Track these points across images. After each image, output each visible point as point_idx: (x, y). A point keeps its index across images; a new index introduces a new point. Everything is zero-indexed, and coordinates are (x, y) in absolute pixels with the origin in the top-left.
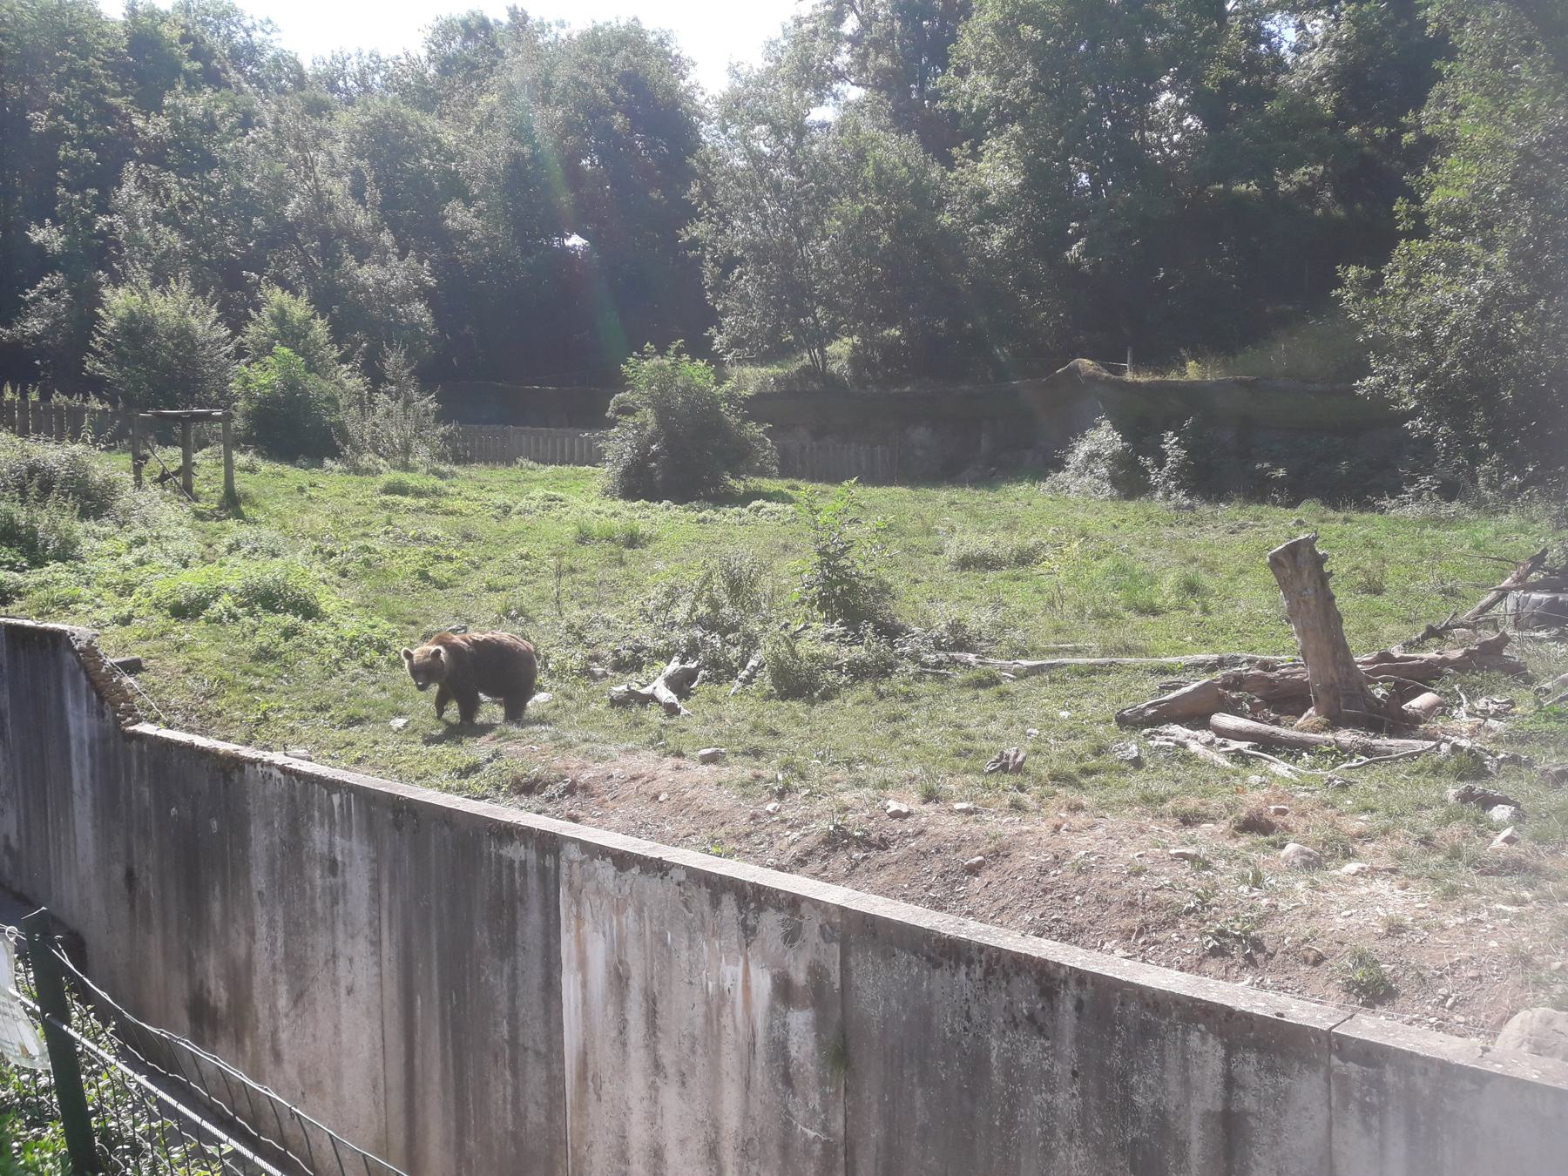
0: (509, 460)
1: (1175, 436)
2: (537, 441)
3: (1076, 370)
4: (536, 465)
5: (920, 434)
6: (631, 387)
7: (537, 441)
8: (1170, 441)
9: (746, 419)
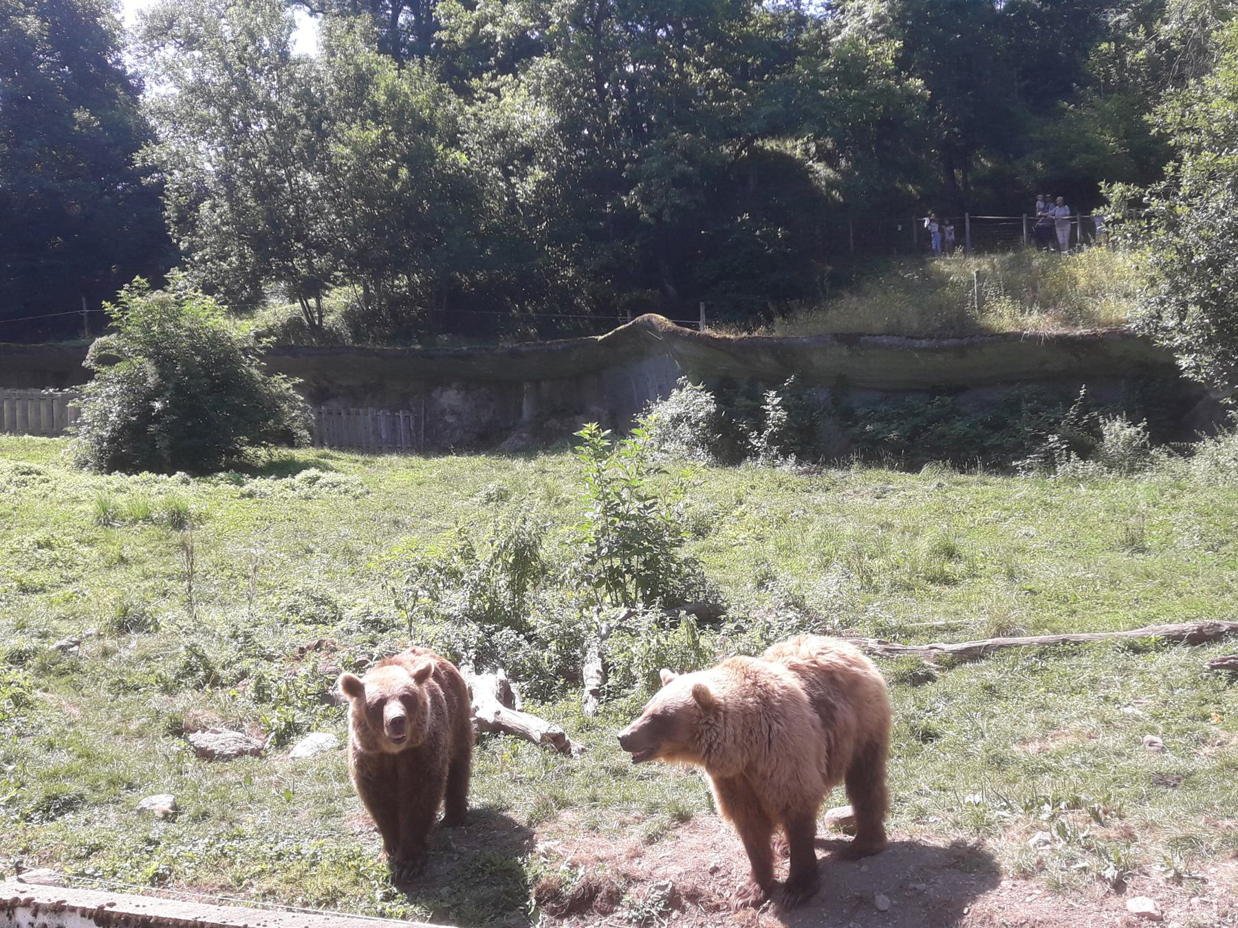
1: (777, 396)
8: (772, 399)
9: (269, 372)
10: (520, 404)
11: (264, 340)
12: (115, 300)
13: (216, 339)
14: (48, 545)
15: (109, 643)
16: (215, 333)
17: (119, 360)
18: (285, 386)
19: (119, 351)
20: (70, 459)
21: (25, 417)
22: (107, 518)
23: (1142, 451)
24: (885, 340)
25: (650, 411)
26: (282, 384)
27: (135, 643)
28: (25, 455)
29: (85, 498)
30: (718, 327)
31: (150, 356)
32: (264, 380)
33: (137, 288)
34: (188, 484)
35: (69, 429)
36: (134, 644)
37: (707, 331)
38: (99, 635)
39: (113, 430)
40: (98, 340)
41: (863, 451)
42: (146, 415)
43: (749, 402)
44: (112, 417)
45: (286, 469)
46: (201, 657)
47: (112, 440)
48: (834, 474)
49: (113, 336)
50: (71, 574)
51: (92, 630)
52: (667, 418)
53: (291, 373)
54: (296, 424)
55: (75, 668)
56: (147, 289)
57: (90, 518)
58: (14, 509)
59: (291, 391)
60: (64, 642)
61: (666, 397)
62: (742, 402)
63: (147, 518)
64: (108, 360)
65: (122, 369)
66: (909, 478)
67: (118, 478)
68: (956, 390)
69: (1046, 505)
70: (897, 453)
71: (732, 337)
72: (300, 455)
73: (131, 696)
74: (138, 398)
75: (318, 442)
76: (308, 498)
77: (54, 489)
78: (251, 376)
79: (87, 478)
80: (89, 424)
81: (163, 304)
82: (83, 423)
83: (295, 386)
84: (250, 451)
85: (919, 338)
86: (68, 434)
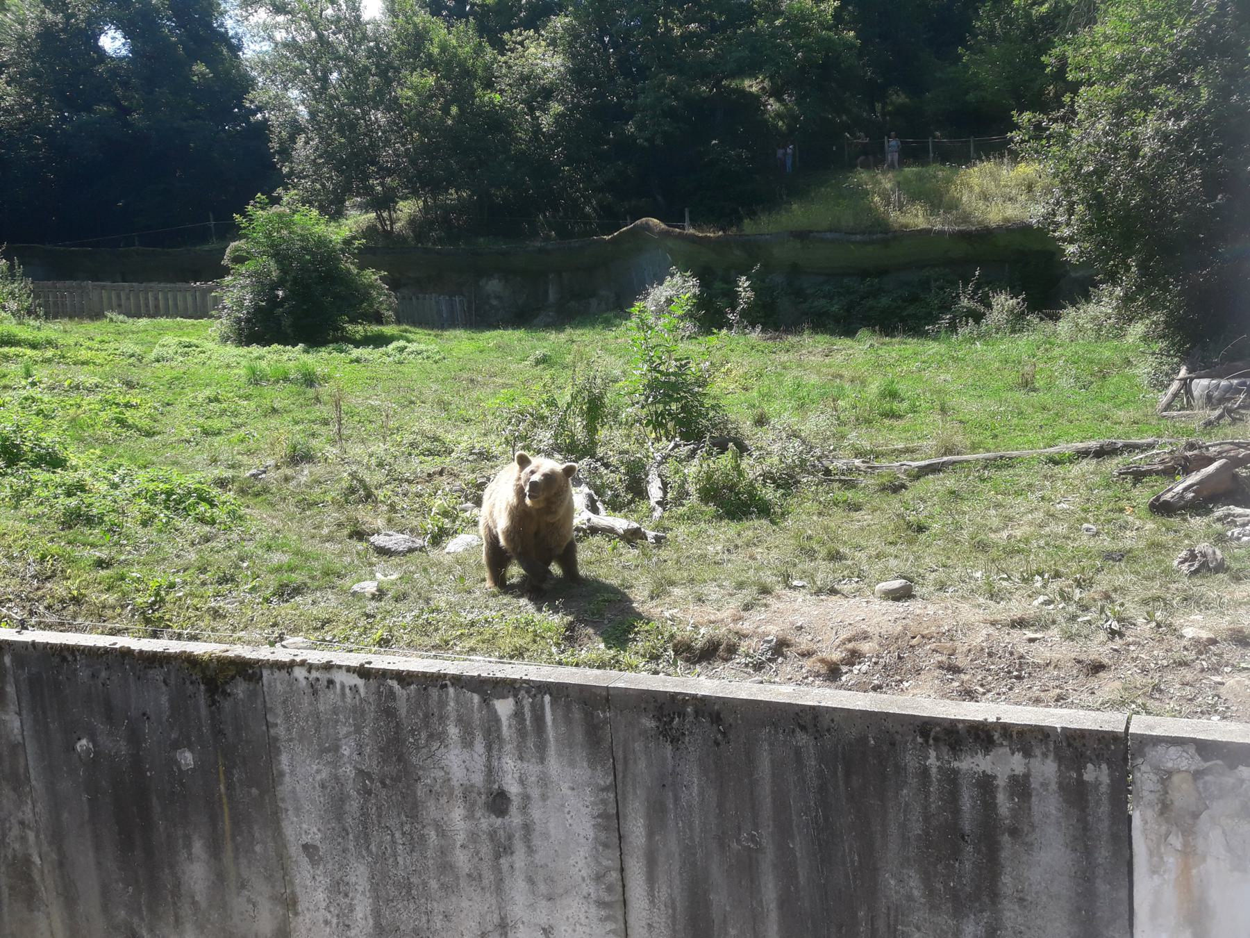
0: (97, 315)
2: (119, 297)
3: (647, 227)
4: (126, 318)
5: (493, 285)
6: (245, 236)
7: (119, 297)
8: (744, 282)
9: (362, 267)
10: (546, 292)
11: (357, 242)
12: (244, 214)
13: (322, 242)
14: (217, 400)
15: (289, 472)
16: (320, 237)
17: (248, 259)
18: (374, 277)
19: (248, 253)
20: (216, 335)
21: (176, 305)
22: (256, 379)
23: (1020, 316)
24: (829, 235)
25: (648, 294)
26: (371, 276)
27: (306, 473)
28: (180, 333)
29: (235, 364)
30: (701, 230)
31: (273, 256)
32: (358, 273)
33: (259, 203)
34: (308, 353)
35: (213, 312)
36: (306, 472)
37: (692, 231)
38: (277, 466)
39: (248, 313)
40: (233, 244)
41: (812, 322)
42: (273, 302)
43: (725, 286)
44: (247, 303)
45: (379, 341)
46: (361, 481)
47: (248, 321)
48: (792, 339)
49: (243, 241)
50: (239, 421)
51: (270, 462)
52: (663, 299)
53: (378, 269)
54: (384, 306)
55: (266, 490)
56: (267, 204)
57: (243, 379)
58: (184, 373)
59: (379, 281)
60: (254, 471)
61: (661, 284)
62: (718, 285)
63: (286, 379)
64: (239, 260)
65: (250, 266)
66: (848, 342)
67: (256, 350)
68: (882, 272)
69: (956, 360)
70: (837, 321)
71: (712, 235)
72: (388, 330)
73: (315, 510)
74: (265, 288)
75: (399, 322)
76: (401, 363)
77: (209, 358)
78: (348, 270)
79: (231, 350)
80: (229, 309)
81: (280, 216)
82: (224, 308)
83: (381, 278)
84: (350, 327)
85: (855, 234)
86: (211, 317)
